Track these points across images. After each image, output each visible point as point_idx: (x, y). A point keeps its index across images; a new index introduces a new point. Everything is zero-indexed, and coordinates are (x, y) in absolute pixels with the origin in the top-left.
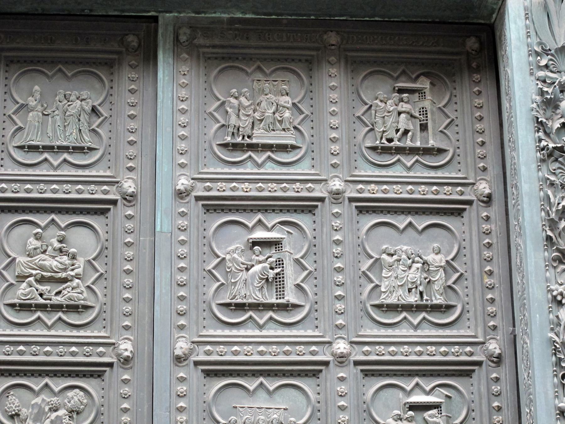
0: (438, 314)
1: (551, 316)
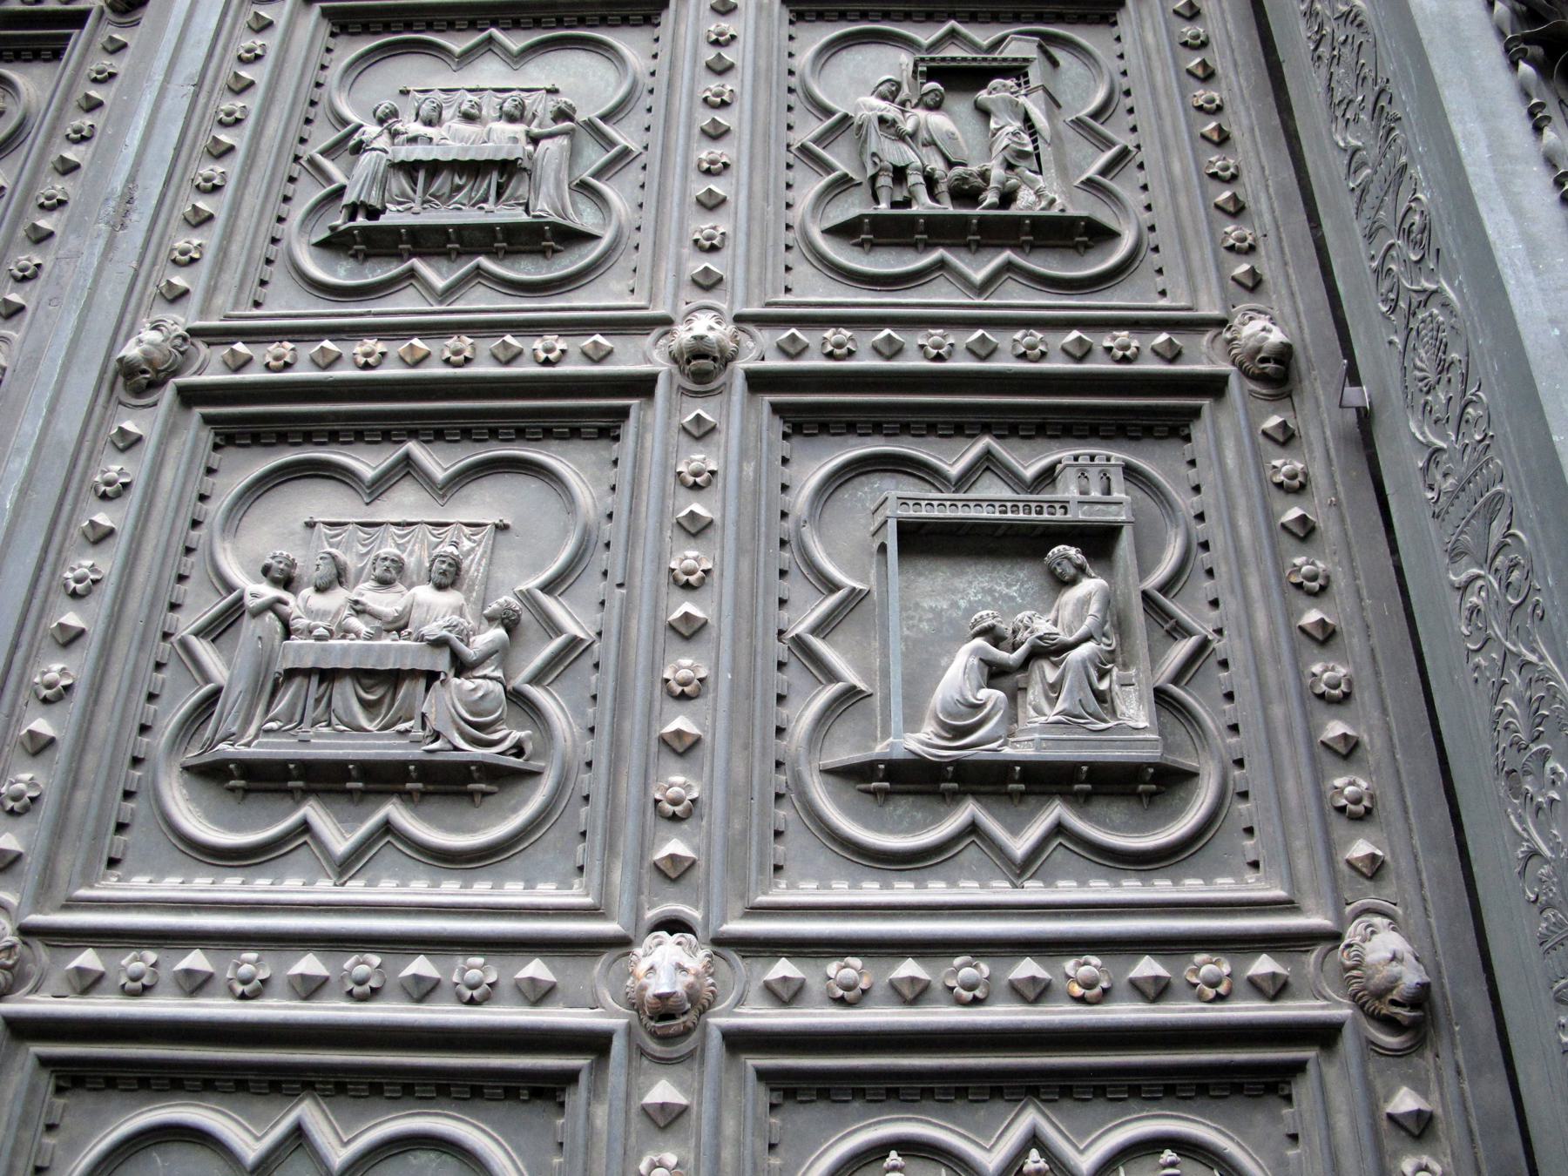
0: (1117, 810)
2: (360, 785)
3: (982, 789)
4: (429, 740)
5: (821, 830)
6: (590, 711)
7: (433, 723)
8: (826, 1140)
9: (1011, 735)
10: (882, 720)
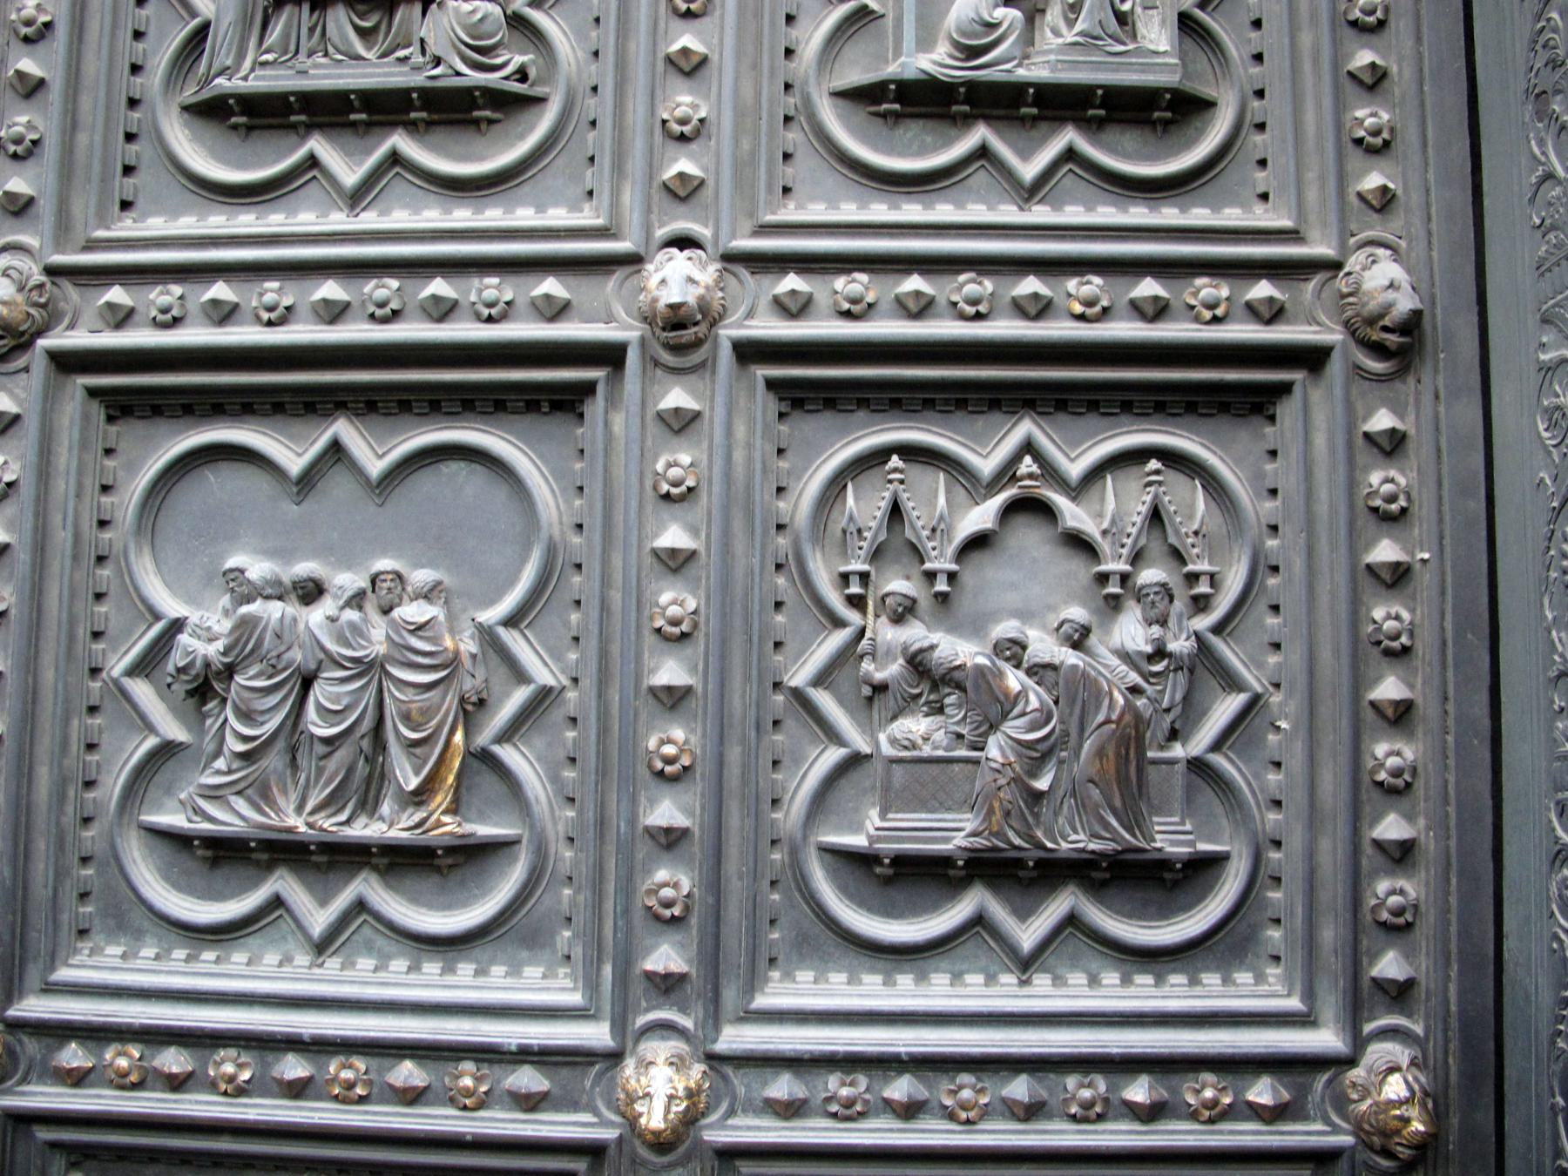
0: (1129, 138)
2: (363, 116)
3: (996, 112)
4: (429, 66)
5: (831, 153)
6: (594, 34)
7: (433, 49)
8: (832, 445)
9: (1027, 57)
10: (894, 41)
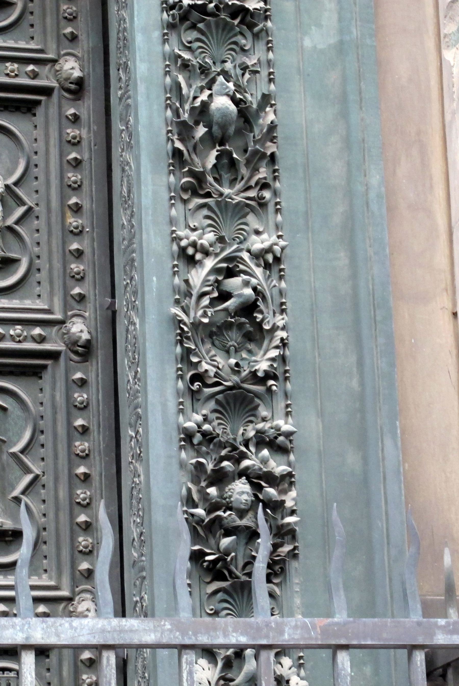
1: (177, 280)
